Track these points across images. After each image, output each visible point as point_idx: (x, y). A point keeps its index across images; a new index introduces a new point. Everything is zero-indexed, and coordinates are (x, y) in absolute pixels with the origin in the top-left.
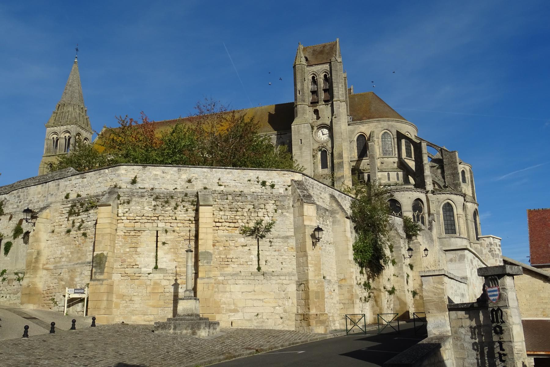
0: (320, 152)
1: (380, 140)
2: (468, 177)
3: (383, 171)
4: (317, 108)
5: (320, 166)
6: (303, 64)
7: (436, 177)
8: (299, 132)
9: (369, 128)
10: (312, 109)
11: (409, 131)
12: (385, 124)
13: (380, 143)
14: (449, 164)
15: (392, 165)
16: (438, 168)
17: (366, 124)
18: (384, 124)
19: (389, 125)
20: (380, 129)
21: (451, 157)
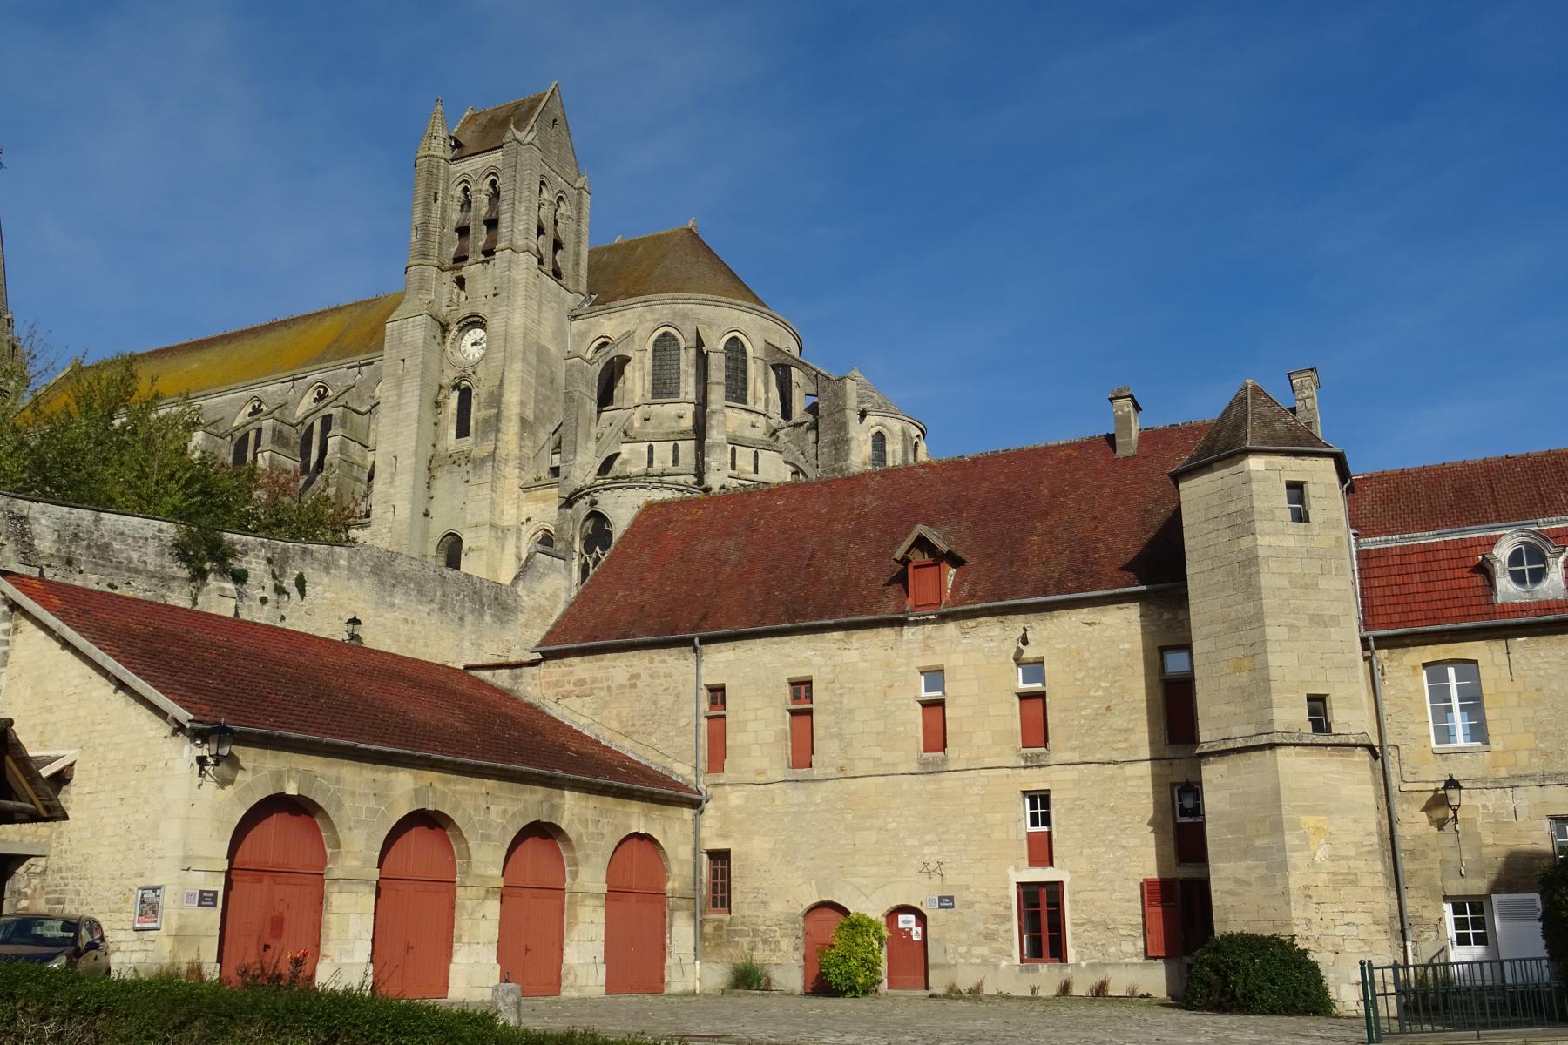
0: (457, 393)
1: (649, 354)
2: (894, 451)
3: (638, 439)
4: (464, 272)
5: (453, 432)
6: (432, 156)
7: (803, 454)
8: (401, 339)
9: (623, 323)
10: (448, 277)
11: (741, 328)
12: (664, 312)
13: (648, 364)
14: (828, 415)
15: (674, 424)
16: (808, 429)
17: (617, 314)
18: (662, 309)
19: (675, 314)
20: (652, 325)
21: (835, 394)
